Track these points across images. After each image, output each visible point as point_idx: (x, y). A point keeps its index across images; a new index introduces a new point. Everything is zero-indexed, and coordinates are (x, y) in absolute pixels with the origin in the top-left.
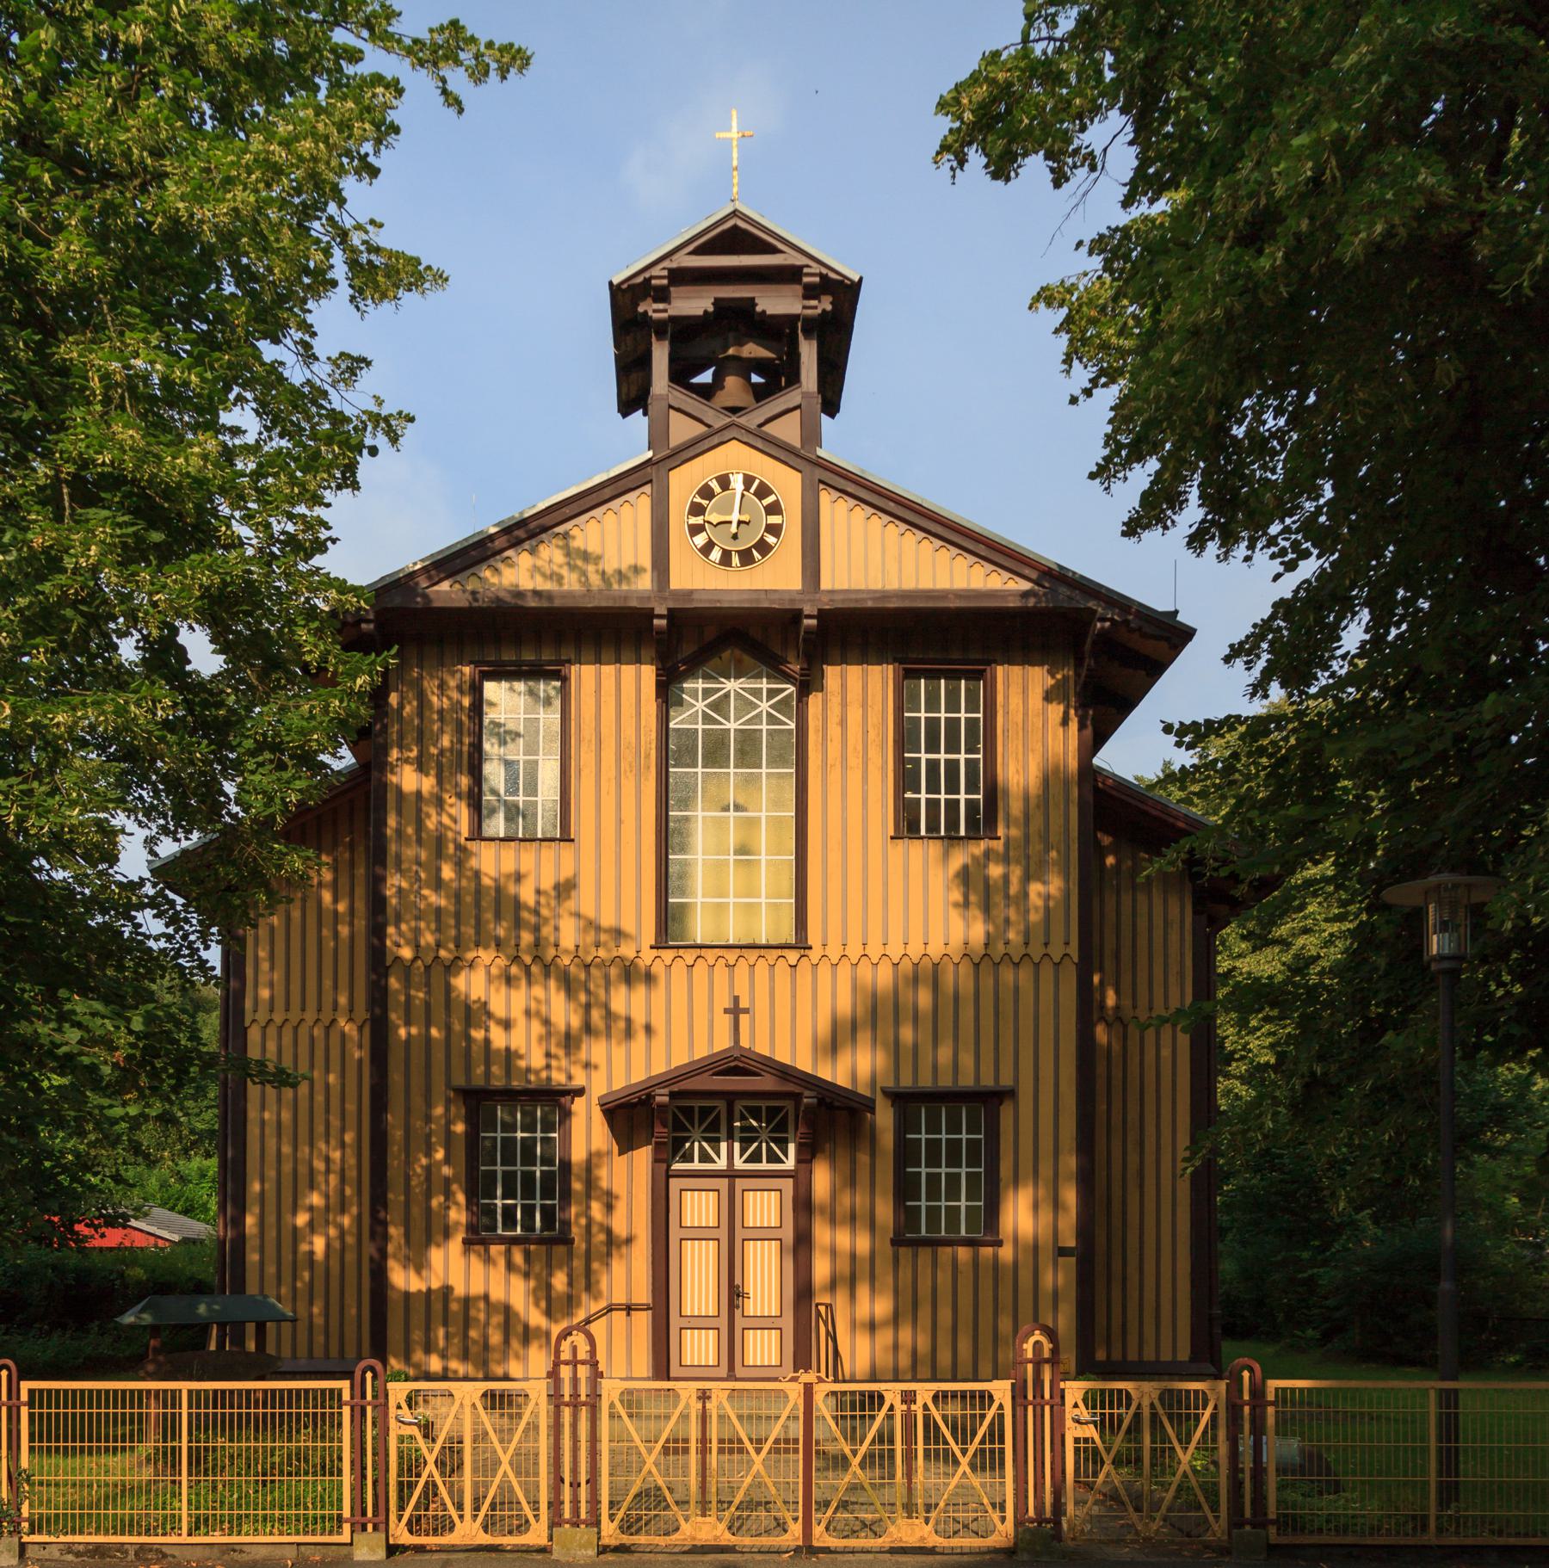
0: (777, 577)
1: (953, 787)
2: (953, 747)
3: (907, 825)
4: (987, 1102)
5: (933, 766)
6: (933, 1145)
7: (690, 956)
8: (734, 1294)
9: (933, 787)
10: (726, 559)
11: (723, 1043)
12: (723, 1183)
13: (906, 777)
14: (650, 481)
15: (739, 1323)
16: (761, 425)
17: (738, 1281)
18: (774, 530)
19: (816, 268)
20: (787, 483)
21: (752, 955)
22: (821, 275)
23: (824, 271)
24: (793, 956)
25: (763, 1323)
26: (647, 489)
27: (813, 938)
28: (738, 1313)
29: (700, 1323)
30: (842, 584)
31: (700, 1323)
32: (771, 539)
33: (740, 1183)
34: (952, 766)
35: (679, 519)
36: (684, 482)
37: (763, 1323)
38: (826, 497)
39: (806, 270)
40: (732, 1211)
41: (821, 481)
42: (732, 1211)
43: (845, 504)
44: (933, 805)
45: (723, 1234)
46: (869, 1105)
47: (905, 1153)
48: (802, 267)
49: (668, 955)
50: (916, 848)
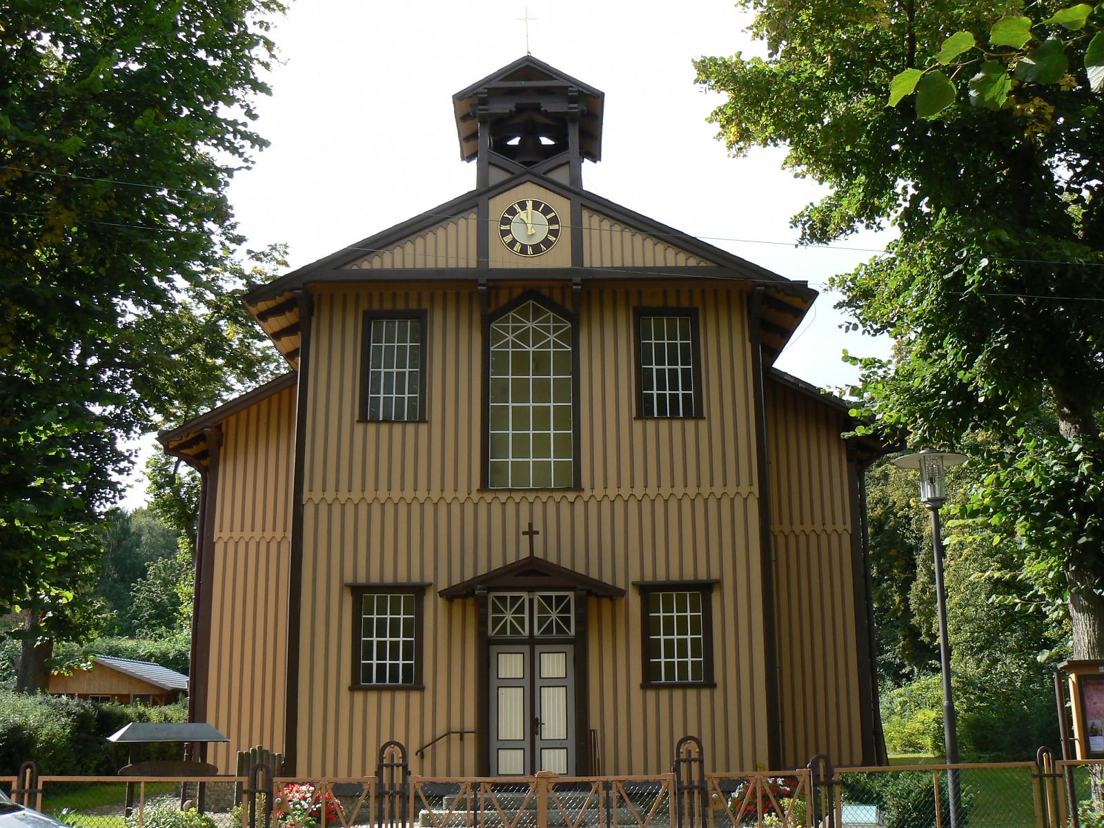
0: (559, 258)
1: (674, 386)
2: (673, 361)
3: (644, 410)
4: (704, 589)
5: (661, 373)
6: (669, 621)
7: (503, 497)
8: (534, 724)
9: (661, 386)
10: (524, 249)
11: (525, 554)
12: (526, 649)
13: (643, 380)
14: (477, 206)
15: (538, 744)
16: (545, 173)
17: (537, 715)
18: (555, 233)
19: (576, 88)
20: (562, 207)
21: (544, 496)
22: (579, 91)
23: (581, 89)
24: (571, 496)
25: (554, 745)
26: (475, 210)
27: (585, 482)
28: (537, 737)
29: (511, 745)
30: (596, 264)
31: (511, 745)
32: (552, 238)
33: (538, 648)
34: (673, 373)
35: (494, 228)
36: (498, 206)
37: (554, 745)
38: (585, 214)
39: (570, 89)
40: (532, 667)
41: (582, 205)
42: (532, 667)
43: (596, 219)
44: (661, 398)
45: (527, 683)
46: (622, 593)
47: (649, 626)
48: (567, 88)
49: (488, 497)
50: (651, 425)
